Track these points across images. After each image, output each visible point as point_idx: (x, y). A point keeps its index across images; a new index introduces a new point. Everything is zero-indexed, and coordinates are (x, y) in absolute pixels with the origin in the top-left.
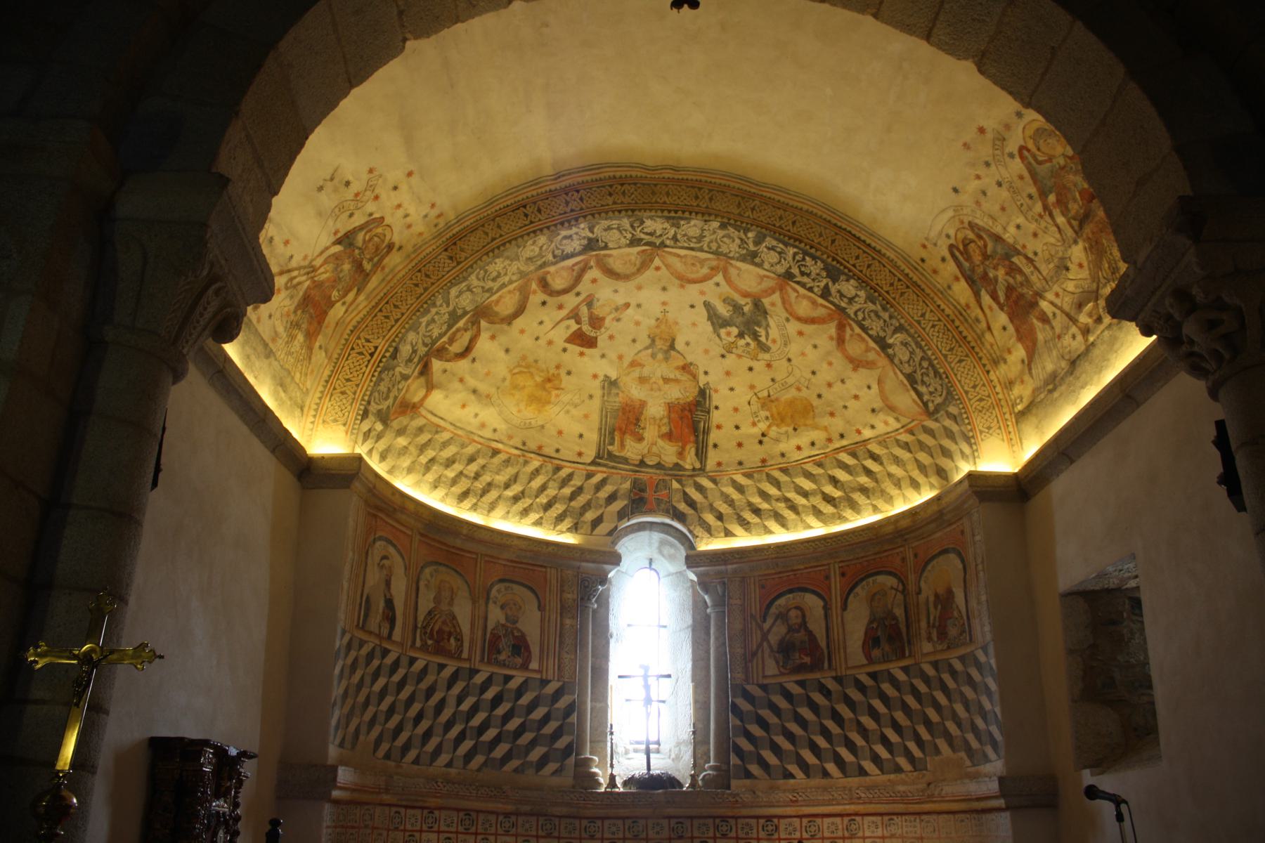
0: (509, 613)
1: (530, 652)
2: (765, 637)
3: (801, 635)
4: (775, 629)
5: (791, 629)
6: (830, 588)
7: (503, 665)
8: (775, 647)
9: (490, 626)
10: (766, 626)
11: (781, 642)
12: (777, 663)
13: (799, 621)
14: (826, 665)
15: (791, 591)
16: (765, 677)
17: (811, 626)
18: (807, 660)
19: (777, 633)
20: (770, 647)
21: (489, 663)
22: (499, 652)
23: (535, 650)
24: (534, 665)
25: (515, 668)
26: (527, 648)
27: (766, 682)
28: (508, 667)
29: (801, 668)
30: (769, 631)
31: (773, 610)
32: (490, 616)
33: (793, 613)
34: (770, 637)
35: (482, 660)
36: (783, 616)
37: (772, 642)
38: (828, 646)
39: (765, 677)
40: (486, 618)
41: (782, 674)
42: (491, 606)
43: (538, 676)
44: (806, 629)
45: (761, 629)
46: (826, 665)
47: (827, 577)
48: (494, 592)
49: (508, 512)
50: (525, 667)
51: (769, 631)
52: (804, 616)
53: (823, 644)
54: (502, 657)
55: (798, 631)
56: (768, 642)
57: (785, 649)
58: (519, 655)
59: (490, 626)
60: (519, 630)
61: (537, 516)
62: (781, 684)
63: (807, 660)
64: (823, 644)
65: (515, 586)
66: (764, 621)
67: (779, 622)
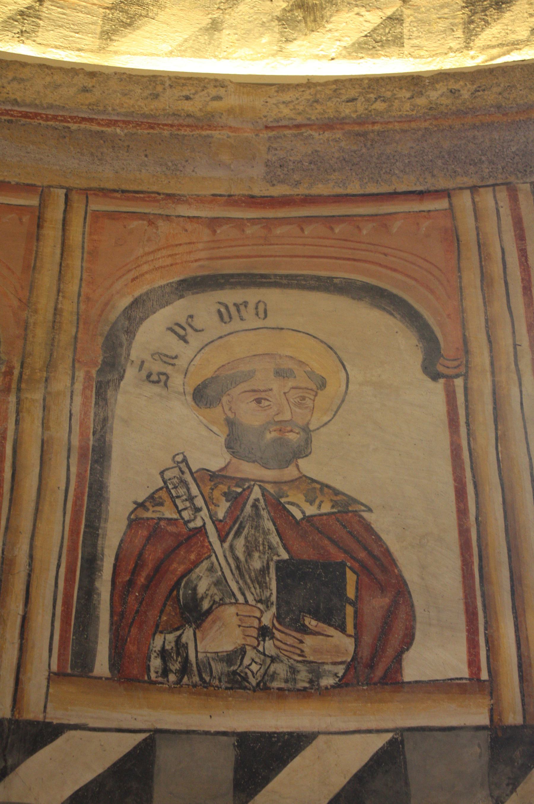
0: (250, 416)
1: (401, 591)
7: (234, 681)
9: (126, 487)
21: (128, 674)
22: (194, 614)
23: (433, 576)
24: (436, 653)
25: (312, 691)
26: (382, 571)
28: (263, 689)
32: (124, 443)
35: (75, 665)
40: (98, 455)
42: (131, 397)
43: (474, 714)
48: (152, 334)
49: (215, 26)
50: (376, 671)
54: (221, 636)
58: (331, 616)
59: (126, 487)
60: (315, 488)
61: (373, 19)
65: (273, 296)
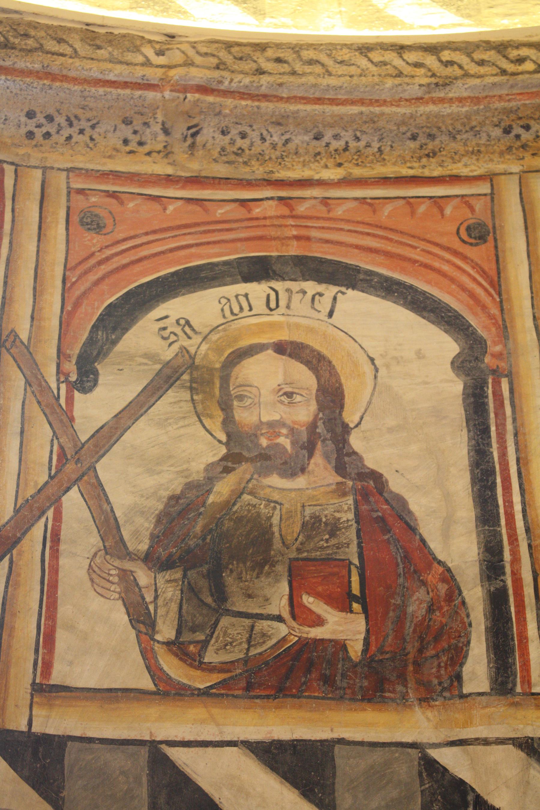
2: (77, 462)
3: (314, 487)
4: (142, 434)
5: (240, 449)
6: (497, 282)
8: (138, 533)
10: (93, 410)
11: (179, 509)
12: (142, 620)
13: (304, 412)
14: (477, 669)
15: (258, 270)
16: (46, 690)
17: (373, 449)
18: (345, 628)
19: (159, 458)
20: (108, 525)
27: (53, 722)
29: (297, 672)
30: (108, 436)
31: (144, 337)
33: (264, 374)
34: (108, 469)
36: (203, 379)
37: (121, 499)
38: (492, 565)
39: (46, 690)
41: (168, 691)
44: (344, 459)
45: (62, 418)
46: (477, 669)
47: (482, 233)
51: (108, 436)
52: (331, 397)
53: (457, 547)
55: (293, 468)
56: (97, 496)
57: (205, 554)
62: (156, 755)
63: (345, 628)
64: (457, 547)
66: (86, 378)
67: (174, 401)
